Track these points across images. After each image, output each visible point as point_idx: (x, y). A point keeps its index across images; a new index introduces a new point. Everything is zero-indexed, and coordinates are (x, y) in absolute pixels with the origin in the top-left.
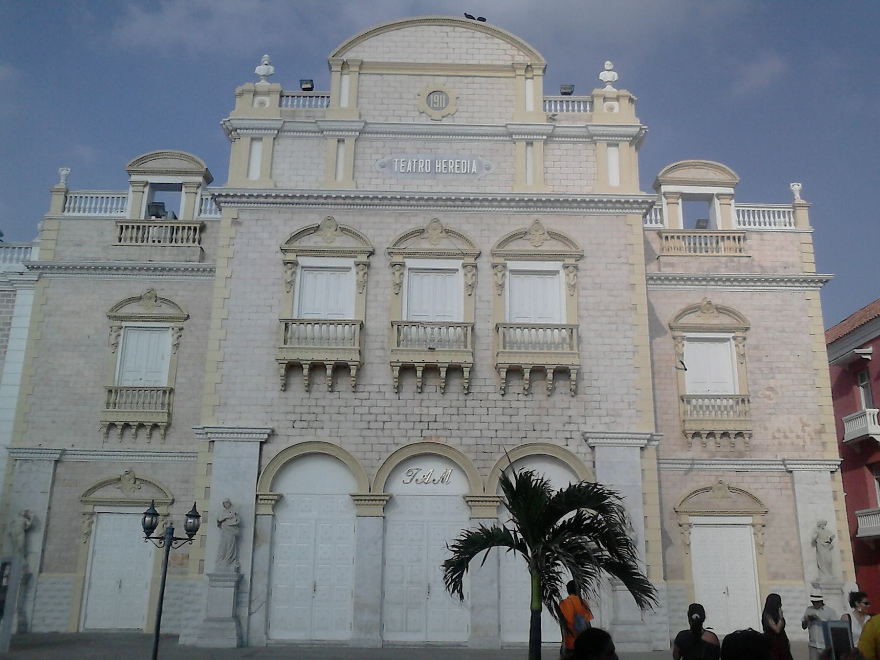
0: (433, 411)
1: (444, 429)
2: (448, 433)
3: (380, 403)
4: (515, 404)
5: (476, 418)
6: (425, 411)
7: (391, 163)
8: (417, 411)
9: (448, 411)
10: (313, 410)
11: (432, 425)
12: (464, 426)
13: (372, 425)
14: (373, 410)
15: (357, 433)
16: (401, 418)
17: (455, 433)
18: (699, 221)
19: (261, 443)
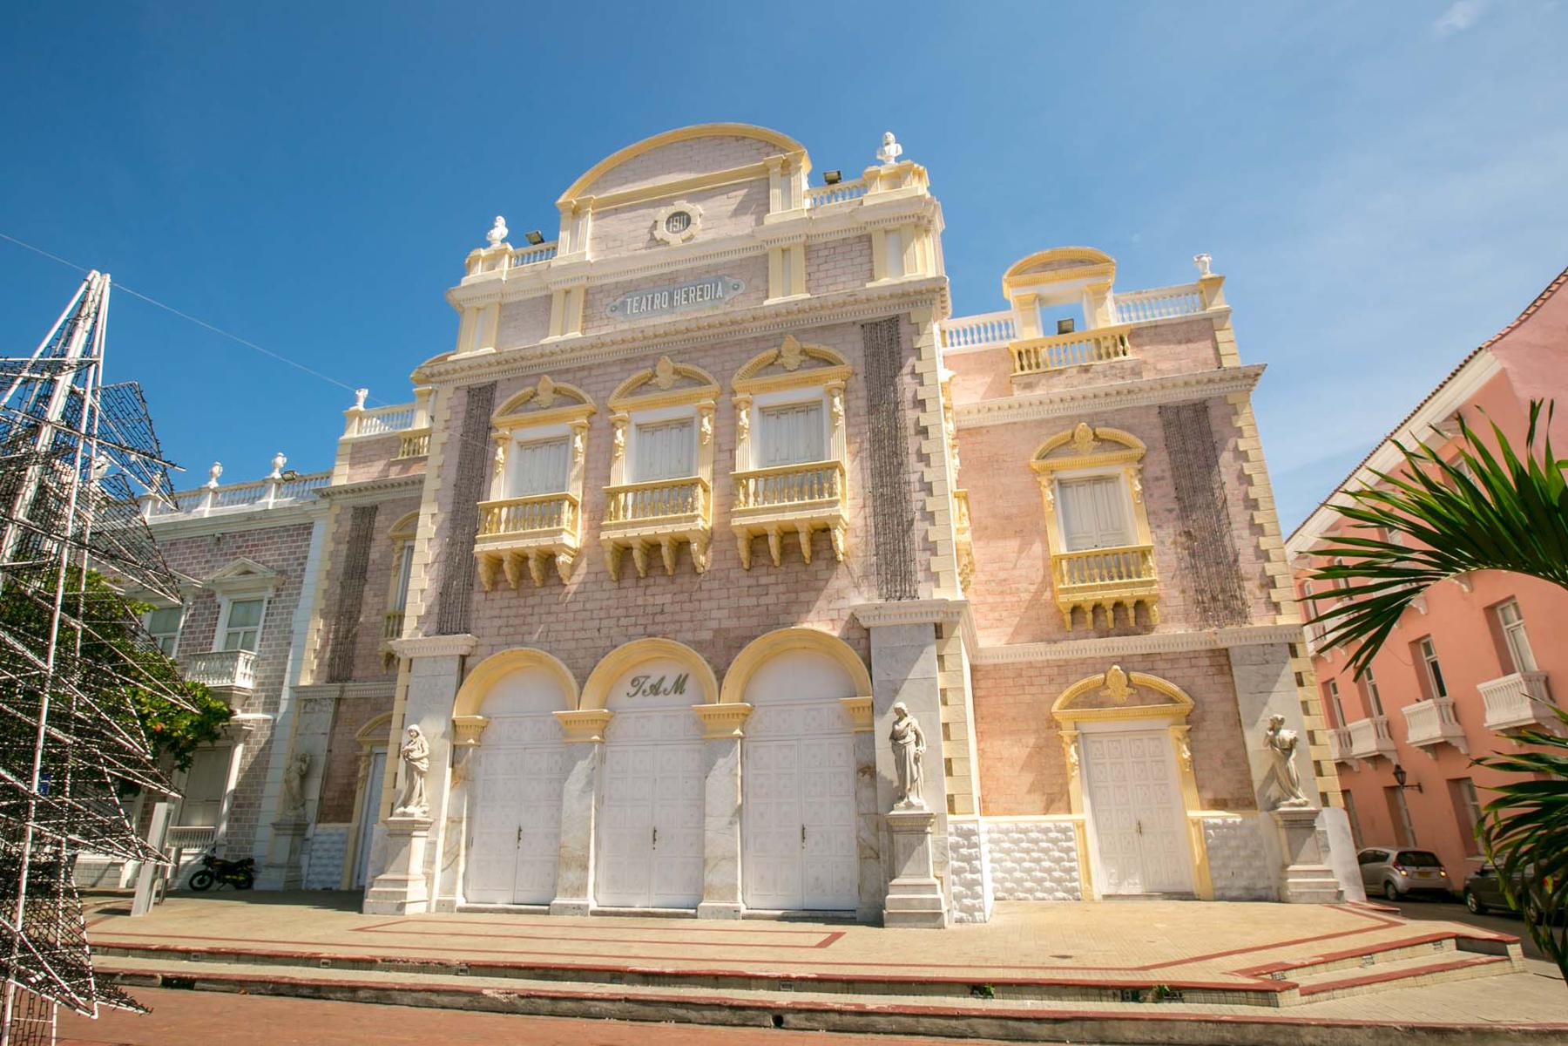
0: (659, 600)
1: (673, 622)
2: (677, 626)
3: (598, 595)
4: (763, 580)
5: (714, 604)
6: (651, 600)
7: (624, 303)
8: (640, 601)
9: (677, 598)
10: (522, 611)
11: (659, 618)
12: (699, 616)
13: (589, 624)
14: (588, 606)
15: (569, 635)
16: (621, 612)
17: (686, 626)
18: (1060, 323)
19: (463, 658)
